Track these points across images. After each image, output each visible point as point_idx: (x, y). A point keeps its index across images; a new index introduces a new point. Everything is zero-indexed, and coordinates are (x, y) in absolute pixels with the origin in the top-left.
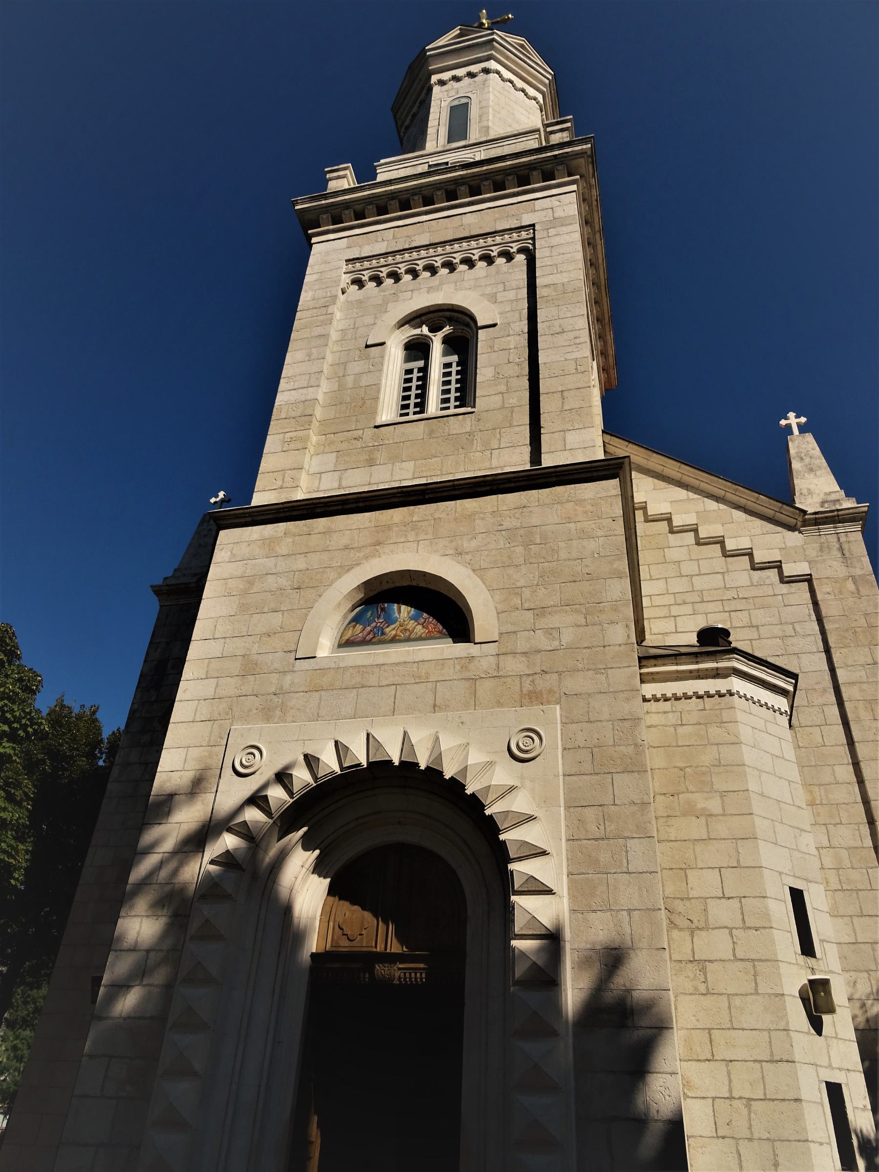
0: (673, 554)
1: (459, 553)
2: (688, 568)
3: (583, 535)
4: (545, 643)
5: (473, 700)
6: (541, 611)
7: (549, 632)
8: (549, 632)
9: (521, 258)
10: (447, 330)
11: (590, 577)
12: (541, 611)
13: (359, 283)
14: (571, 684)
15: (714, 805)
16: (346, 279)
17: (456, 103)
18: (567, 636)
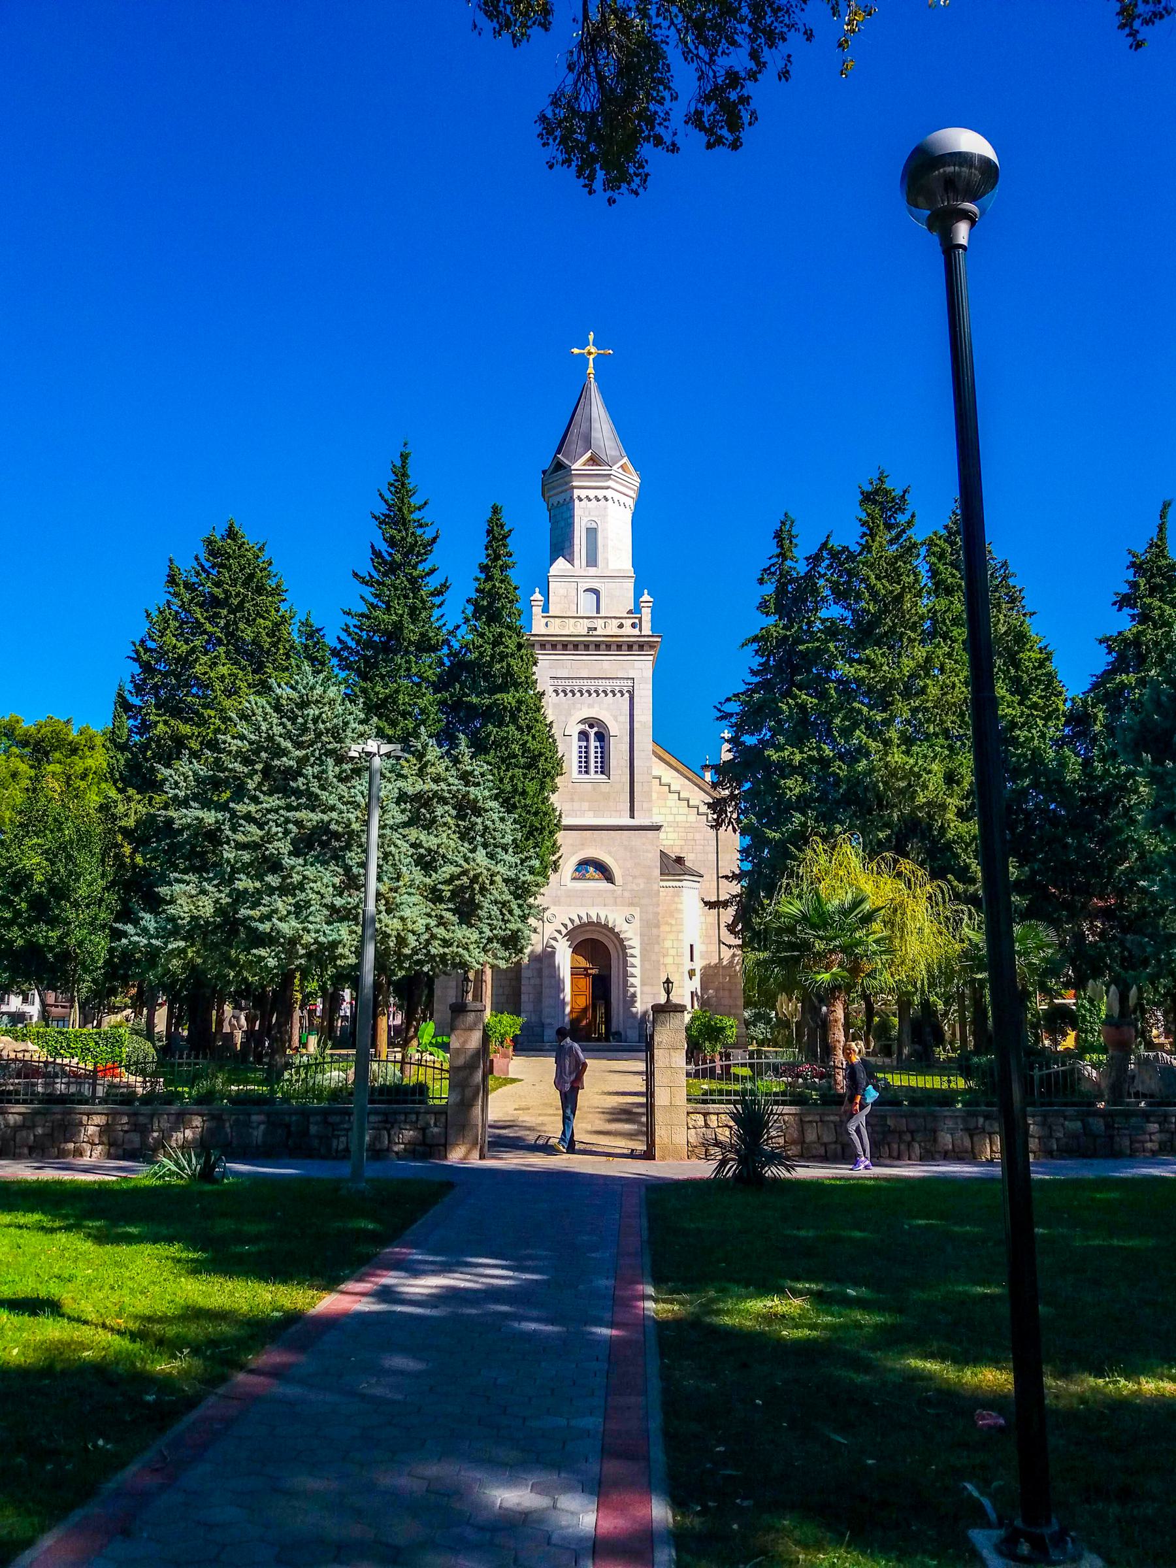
0: (669, 803)
1: (610, 853)
2: (675, 811)
3: (647, 851)
4: (636, 888)
5: (616, 904)
6: (635, 877)
7: (638, 884)
8: (638, 884)
9: (627, 695)
10: (595, 729)
11: (649, 867)
12: (635, 877)
13: (556, 691)
14: (644, 901)
15: (673, 922)
16: (552, 689)
17: (589, 526)
18: (642, 886)
